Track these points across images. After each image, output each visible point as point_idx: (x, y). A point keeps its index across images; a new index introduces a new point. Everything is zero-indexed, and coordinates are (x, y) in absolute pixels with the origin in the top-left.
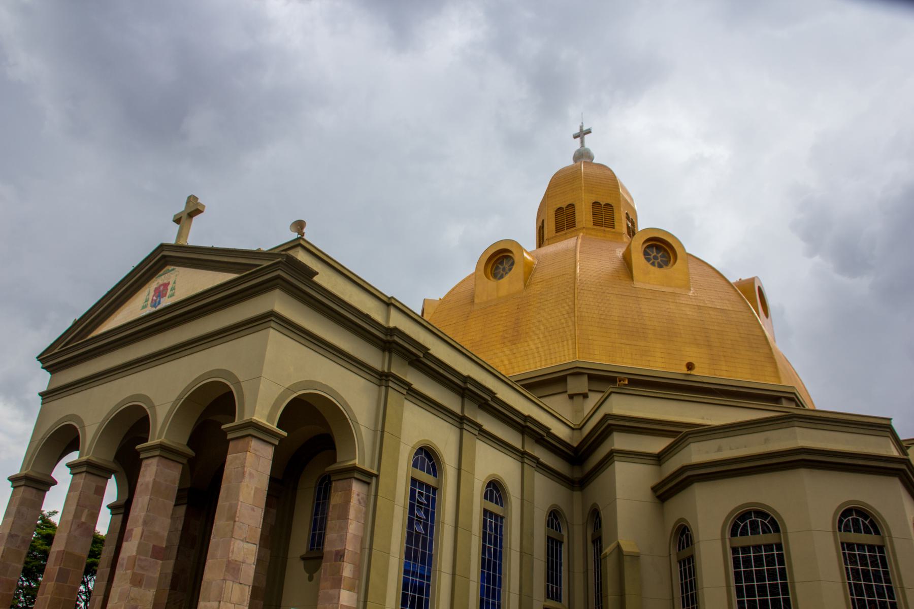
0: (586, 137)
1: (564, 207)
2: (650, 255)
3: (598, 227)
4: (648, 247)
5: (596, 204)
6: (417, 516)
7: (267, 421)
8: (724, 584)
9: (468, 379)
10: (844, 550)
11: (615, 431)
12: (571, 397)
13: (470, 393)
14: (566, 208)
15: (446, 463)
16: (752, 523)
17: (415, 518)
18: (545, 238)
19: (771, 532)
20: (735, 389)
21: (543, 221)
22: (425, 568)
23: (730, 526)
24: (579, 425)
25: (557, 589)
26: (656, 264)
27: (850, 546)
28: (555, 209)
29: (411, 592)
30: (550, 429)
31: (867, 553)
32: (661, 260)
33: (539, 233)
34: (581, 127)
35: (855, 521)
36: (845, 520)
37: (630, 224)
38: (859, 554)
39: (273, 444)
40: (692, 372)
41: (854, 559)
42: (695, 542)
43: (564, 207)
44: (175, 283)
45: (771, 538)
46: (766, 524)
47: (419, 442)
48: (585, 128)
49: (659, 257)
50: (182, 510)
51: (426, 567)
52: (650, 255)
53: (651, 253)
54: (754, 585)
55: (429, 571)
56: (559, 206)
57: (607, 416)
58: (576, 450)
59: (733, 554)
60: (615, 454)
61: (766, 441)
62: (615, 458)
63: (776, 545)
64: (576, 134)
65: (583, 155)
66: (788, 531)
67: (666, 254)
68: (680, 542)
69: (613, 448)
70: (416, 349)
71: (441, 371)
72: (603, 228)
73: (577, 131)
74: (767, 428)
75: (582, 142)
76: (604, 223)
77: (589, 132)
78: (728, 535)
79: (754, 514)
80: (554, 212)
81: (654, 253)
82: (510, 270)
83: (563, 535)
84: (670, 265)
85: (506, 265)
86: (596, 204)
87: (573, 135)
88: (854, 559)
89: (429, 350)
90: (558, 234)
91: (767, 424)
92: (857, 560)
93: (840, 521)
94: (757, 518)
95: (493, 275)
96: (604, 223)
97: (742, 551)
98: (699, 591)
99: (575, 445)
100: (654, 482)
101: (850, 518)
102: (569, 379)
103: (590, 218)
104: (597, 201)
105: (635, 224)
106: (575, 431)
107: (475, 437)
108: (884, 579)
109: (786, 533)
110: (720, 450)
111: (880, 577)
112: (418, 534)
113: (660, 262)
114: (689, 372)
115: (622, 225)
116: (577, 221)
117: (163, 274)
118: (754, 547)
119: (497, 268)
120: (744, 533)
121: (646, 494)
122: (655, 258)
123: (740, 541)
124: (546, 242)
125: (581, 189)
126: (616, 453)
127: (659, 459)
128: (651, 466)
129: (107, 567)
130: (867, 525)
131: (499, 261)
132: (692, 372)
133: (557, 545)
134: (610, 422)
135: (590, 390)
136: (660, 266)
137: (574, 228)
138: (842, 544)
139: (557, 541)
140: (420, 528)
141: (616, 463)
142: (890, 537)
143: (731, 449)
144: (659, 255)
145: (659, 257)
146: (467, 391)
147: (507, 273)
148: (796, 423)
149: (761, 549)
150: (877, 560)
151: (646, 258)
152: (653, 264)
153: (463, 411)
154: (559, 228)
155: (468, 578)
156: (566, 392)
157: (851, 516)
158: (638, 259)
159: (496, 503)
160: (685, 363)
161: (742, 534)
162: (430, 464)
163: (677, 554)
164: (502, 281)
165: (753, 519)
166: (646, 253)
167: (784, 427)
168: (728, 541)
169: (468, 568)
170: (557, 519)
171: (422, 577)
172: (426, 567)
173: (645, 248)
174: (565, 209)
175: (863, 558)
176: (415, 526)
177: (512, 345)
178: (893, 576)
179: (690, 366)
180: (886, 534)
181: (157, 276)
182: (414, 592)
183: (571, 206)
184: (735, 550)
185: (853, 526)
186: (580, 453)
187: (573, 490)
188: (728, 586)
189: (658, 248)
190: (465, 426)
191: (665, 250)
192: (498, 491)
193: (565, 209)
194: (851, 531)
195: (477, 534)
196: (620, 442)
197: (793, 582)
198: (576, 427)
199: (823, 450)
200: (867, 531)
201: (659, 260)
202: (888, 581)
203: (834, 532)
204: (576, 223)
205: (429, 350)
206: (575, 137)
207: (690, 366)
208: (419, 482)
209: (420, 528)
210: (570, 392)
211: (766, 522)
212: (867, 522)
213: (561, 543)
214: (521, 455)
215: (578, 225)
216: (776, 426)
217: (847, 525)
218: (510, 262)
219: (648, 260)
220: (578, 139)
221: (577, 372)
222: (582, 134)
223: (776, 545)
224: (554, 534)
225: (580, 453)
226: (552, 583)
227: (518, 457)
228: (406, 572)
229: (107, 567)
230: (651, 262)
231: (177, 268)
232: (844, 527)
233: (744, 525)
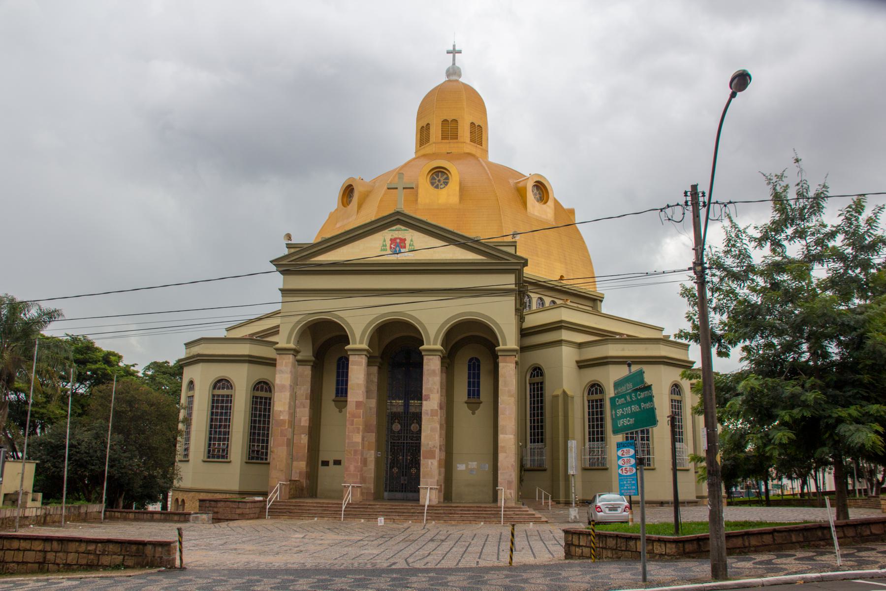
44: (412, 241)
48: (457, 48)
50: (375, 369)
65: (453, 72)
77: (460, 52)
90: (444, 141)
100: (578, 359)
117: (394, 230)
127: (580, 345)
129: (306, 399)
137: (455, 141)
181: (389, 229)
196: (565, 335)
206: (448, 52)
222: (454, 52)
229: (306, 399)
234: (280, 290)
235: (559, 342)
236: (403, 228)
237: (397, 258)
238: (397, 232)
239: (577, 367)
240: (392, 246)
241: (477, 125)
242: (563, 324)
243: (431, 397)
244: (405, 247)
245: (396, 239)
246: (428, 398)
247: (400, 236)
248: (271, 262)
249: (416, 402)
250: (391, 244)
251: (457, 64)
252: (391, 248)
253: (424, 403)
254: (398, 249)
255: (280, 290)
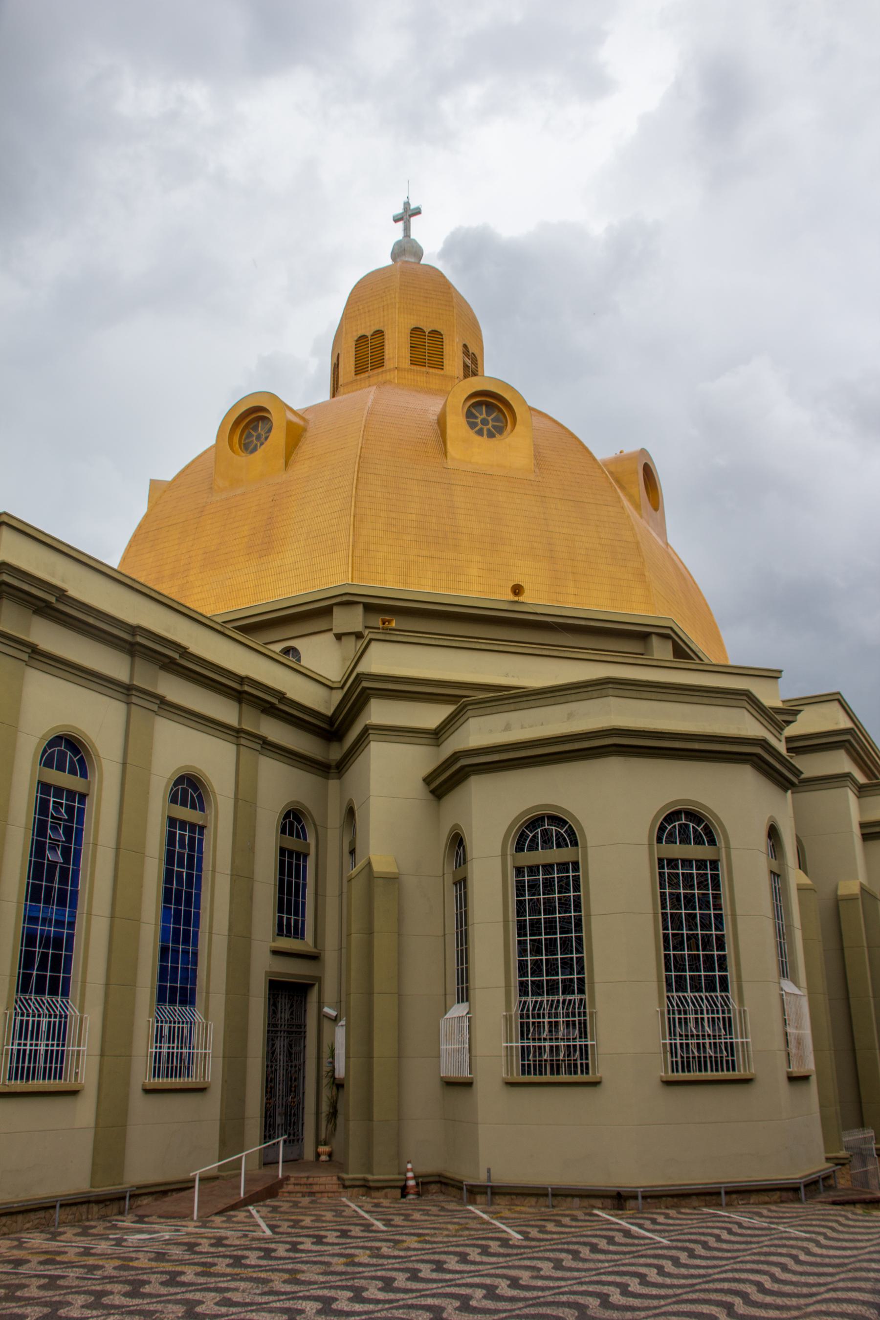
0: (413, 219)
1: (369, 334)
2: (476, 418)
3: (418, 368)
4: (475, 405)
5: (416, 331)
6: (50, 838)
8: (501, 919)
9: (138, 629)
10: (663, 868)
11: (374, 698)
12: (339, 637)
13: (143, 650)
14: (372, 336)
15: (101, 755)
16: (545, 833)
17: (48, 841)
18: (340, 384)
19: (567, 846)
20: (583, 623)
21: (339, 354)
22: (65, 911)
23: (514, 837)
24: (340, 682)
25: (296, 921)
26: (485, 432)
27: (672, 863)
28: (356, 338)
29: (39, 948)
30: (284, 694)
31: (694, 871)
32: (494, 427)
33: (334, 374)
34: (407, 205)
35: (684, 828)
36: (669, 828)
37: (469, 362)
38: (683, 874)
40: (521, 599)
41: (675, 881)
42: (469, 859)
43: (369, 334)
46: (562, 835)
47: (52, 729)
48: (413, 206)
49: (490, 422)
51: (68, 909)
52: (476, 418)
53: (478, 415)
54: (541, 919)
55: (73, 915)
56: (361, 333)
57: (361, 676)
58: (331, 720)
59: (517, 876)
60: (370, 731)
61: (570, 716)
62: (371, 737)
63: (572, 863)
64: (397, 215)
66: (589, 845)
67: (501, 416)
68: (457, 856)
69: (367, 722)
70: (42, 592)
71: (91, 621)
72: (424, 369)
73: (400, 210)
74: (573, 697)
75: (407, 230)
76: (427, 361)
77: (417, 212)
78: (511, 849)
79: (548, 819)
80: (354, 343)
81: (482, 414)
82: (266, 438)
83: (309, 844)
84: (505, 433)
85: (261, 428)
86: (416, 331)
87: (394, 217)
88: (675, 881)
89: (66, 591)
90: (358, 377)
91: (572, 691)
92: (679, 881)
93: (662, 829)
94: (551, 825)
95: (242, 445)
96: (427, 361)
97: (528, 872)
98: (470, 927)
99: (329, 713)
101: (677, 823)
102: (336, 610)
103: (406, 352)
104: (418, 326)
105: (479, 362)
106: (334, 692)
107: (153, 714)
108: (713, 905)
109: (585, 848)
110: (508, 728)
111: (709, 902)
112: (52, 865)
113: (491, 429)
114: (516, 599)
115: (454, 362)
116: (386, 357)
118: (544, 866)
119: (249, 436)
120: (533, 847)
121: (415, 788)
122: (484, 422)
123: (529, 858)
124: (341, 389)
125: (395, 308)
126: (372, 729)
127: (437, 736)
128: (428, 747)
130: (700, 833)
131: (252, 426)
132: (521, 599)
133: (298, 859)
134: (365, 684)
135: (366, 627)
136: (491, 435)
137: (381, 369)
138: (660, 860)
139: (298, 855)
140: (56, 857)
141: (373, 745)
142: (728, 847)
143: (522, 727)
144: (490, 418)
145: (490, 422)
146: (138, 648)
147: (262, 444)
148: (611, 692)
149: (553, 870)
150: (707, 880)
151: (469, 423)
152: (480, 433)
153: (132, 677)
154: (360, 369)
155: (138, 920)
156: (331, 630)
157: (678, 820)
158: (457, 424)
159: (193, 807)
160: (511, 584)
161: (530, 849)
162: (75, 759)
163: (454, 873)
164: (253, 455)
165: (546, 827)
166: (469, 415)
167: (596, 696)
168: (509, 858)
169: (137, 907)
170: (299, 822)
171: (60, 924)
172: (68, 909)
173: (469, 407)
174: (369, 338)
175: (688, 878)
176: (47, 852)
177: (260, 557)
178: (725, 901)
179: (517, 590)
180: (723, 845)
182: (47, 946)
183: (379, 333)
184: (519, 871)
185: (679, 835)
186: (336, 726)
187: (328, 778)
188: (506, 921)
189: (490, 407)
190: (134, 700)
191: (500, 411)
192: (196, 789)
193: (369, 338)
194: (676, 843)
195: (157, 855)
197: (588, 915)
198: (335, 685)
199: (644, 731)
200: (699, 841)
201: (490, 426)
202: (718, 907)
203: (650, 845)
204: (385, 360)
206: (396, 220)
207: (517, 590)
208: (54, 788)
209: (56, 857)
210: (337, 630)
211: (562, 832)
212: (699, 829)
213: (306, 856)
214: (236, 734)
215: (389, 364)
216: (584, 696)
217: (671, 834)
218: (268, 426)
219: (472, 425)
220: (401, 224)
221: (347, 601)
222: (408, 215)
223: (572, 863)
224: (292, 843)
225: (336, 726)
226: (289, 913)
227: (232, 737)
228: (31, 919)
230: (477, 428)
232: (666, 837)
233: (533, 836)
239: (431, 796)
241: (427, 330)
251: (413, 236)
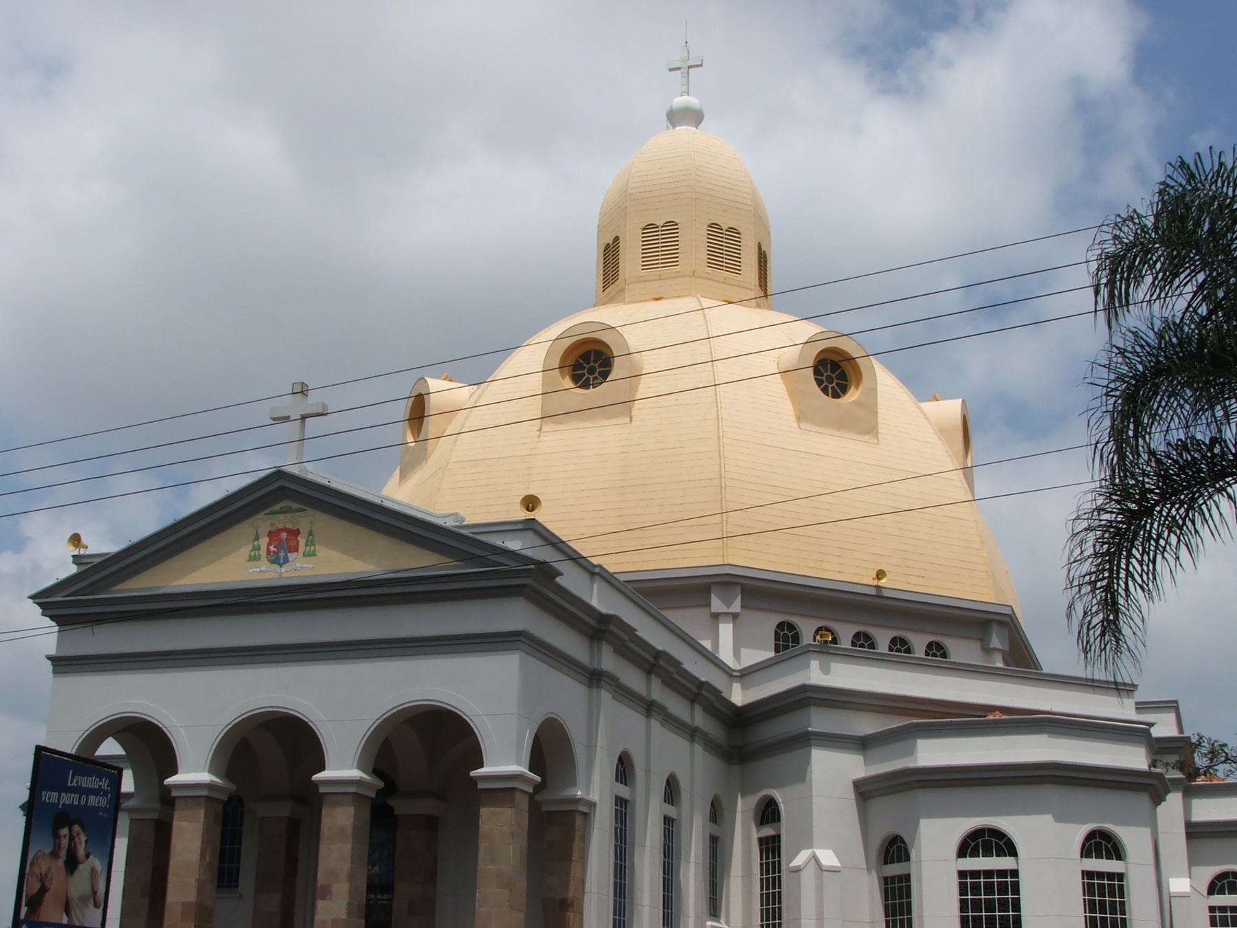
7: (530, 771)
39: (525, 792)
45: (1005, 863)
62: (813, 742)
89: (636, 631)
101: (1093, 841)
117: (276, 513)
157: (1094, 839)
165: (987, 838)
181: (267, 511)
205: (636, 631)
211: (1001, 843)
212: (1109, 846)
231: (310, 511)
234: (49, 658)
235: (805, 740)
236: (295, 506)
237: (281, 574)
238: (281, 517)
240: (272, 548)
241: (725, 227)
242: (809, 694)
243: (333, 890)
244: (296, 549)
245: (280, 531)
246: (327, 893)
247: (289, 526)
248: (32, 597)
249: (379, 897)
250: (269, 544)
252: (269, 552)
253: (320, 904)
254: (282, 554)
255: (49, 658)
